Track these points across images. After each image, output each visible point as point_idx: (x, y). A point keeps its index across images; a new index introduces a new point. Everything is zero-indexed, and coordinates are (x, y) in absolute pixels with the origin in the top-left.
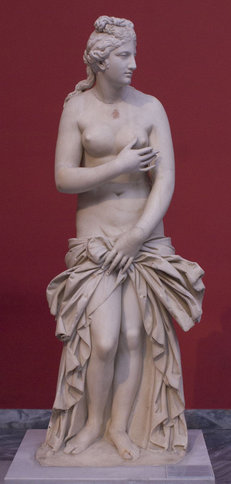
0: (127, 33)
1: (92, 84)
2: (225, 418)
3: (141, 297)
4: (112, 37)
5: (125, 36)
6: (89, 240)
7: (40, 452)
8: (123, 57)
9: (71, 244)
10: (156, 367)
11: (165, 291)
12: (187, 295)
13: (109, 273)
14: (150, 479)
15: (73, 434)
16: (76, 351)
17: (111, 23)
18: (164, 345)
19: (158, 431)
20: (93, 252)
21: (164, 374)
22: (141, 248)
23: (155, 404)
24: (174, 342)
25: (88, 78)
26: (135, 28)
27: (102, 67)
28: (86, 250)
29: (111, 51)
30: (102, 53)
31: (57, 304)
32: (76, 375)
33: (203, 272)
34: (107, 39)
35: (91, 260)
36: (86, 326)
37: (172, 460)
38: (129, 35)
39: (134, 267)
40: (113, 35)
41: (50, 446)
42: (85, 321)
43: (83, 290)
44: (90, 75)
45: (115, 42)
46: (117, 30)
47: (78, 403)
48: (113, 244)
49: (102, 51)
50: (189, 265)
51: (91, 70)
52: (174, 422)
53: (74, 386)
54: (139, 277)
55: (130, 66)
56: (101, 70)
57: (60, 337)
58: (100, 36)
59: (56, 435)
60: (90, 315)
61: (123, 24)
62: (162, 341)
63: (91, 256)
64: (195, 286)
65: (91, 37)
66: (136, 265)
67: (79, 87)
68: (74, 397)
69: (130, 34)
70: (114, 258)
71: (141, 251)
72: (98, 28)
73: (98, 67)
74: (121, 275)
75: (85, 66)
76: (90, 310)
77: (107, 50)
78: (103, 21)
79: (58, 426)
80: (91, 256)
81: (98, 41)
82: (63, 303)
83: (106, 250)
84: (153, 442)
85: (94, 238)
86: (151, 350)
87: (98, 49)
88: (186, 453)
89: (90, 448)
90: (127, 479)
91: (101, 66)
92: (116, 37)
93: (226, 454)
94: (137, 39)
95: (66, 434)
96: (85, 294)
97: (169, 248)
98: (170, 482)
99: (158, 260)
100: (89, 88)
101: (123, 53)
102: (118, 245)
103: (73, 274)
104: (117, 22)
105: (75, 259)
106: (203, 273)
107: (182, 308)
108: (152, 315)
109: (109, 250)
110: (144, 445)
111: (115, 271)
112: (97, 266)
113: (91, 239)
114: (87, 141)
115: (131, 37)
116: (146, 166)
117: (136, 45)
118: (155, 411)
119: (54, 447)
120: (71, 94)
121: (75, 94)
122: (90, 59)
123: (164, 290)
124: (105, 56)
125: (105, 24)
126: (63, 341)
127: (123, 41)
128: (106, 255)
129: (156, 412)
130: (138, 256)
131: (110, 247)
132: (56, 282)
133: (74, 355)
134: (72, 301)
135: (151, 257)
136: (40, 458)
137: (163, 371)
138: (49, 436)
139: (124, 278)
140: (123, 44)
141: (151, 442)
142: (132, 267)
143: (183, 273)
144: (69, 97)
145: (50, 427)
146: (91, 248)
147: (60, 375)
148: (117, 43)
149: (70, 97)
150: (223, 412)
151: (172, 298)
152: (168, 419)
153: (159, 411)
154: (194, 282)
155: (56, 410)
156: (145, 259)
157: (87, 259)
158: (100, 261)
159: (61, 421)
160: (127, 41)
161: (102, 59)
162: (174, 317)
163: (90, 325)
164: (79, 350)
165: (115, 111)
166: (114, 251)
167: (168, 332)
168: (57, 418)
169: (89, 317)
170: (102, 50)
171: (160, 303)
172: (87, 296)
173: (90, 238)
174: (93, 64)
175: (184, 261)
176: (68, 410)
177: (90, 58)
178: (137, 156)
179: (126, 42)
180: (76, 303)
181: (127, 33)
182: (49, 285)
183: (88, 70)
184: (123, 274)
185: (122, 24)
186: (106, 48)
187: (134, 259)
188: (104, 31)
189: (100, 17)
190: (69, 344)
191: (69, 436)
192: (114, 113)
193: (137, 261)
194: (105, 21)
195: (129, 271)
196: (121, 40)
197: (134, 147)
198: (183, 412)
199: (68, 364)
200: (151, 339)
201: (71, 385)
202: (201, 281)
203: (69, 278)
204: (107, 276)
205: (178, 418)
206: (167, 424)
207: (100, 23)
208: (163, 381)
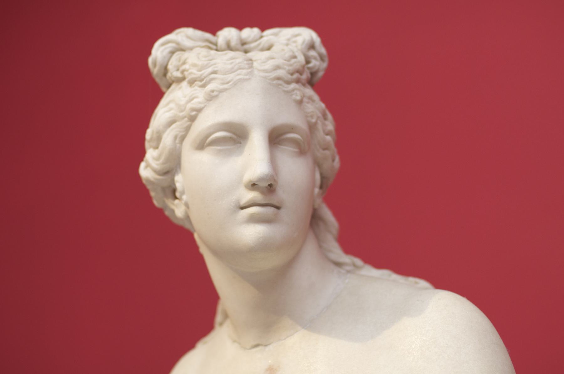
8: (219, 148)
29: (183, 138)
78: (163, 44)
91: (173, 204)
92: (192, 83)
124: (163, 163)
127: (210, 87)
148: (191, 100)
170: (154, 144)
179: (225, 90)
185: (259, 45)
186: (164, 132)
196: (204, 86)
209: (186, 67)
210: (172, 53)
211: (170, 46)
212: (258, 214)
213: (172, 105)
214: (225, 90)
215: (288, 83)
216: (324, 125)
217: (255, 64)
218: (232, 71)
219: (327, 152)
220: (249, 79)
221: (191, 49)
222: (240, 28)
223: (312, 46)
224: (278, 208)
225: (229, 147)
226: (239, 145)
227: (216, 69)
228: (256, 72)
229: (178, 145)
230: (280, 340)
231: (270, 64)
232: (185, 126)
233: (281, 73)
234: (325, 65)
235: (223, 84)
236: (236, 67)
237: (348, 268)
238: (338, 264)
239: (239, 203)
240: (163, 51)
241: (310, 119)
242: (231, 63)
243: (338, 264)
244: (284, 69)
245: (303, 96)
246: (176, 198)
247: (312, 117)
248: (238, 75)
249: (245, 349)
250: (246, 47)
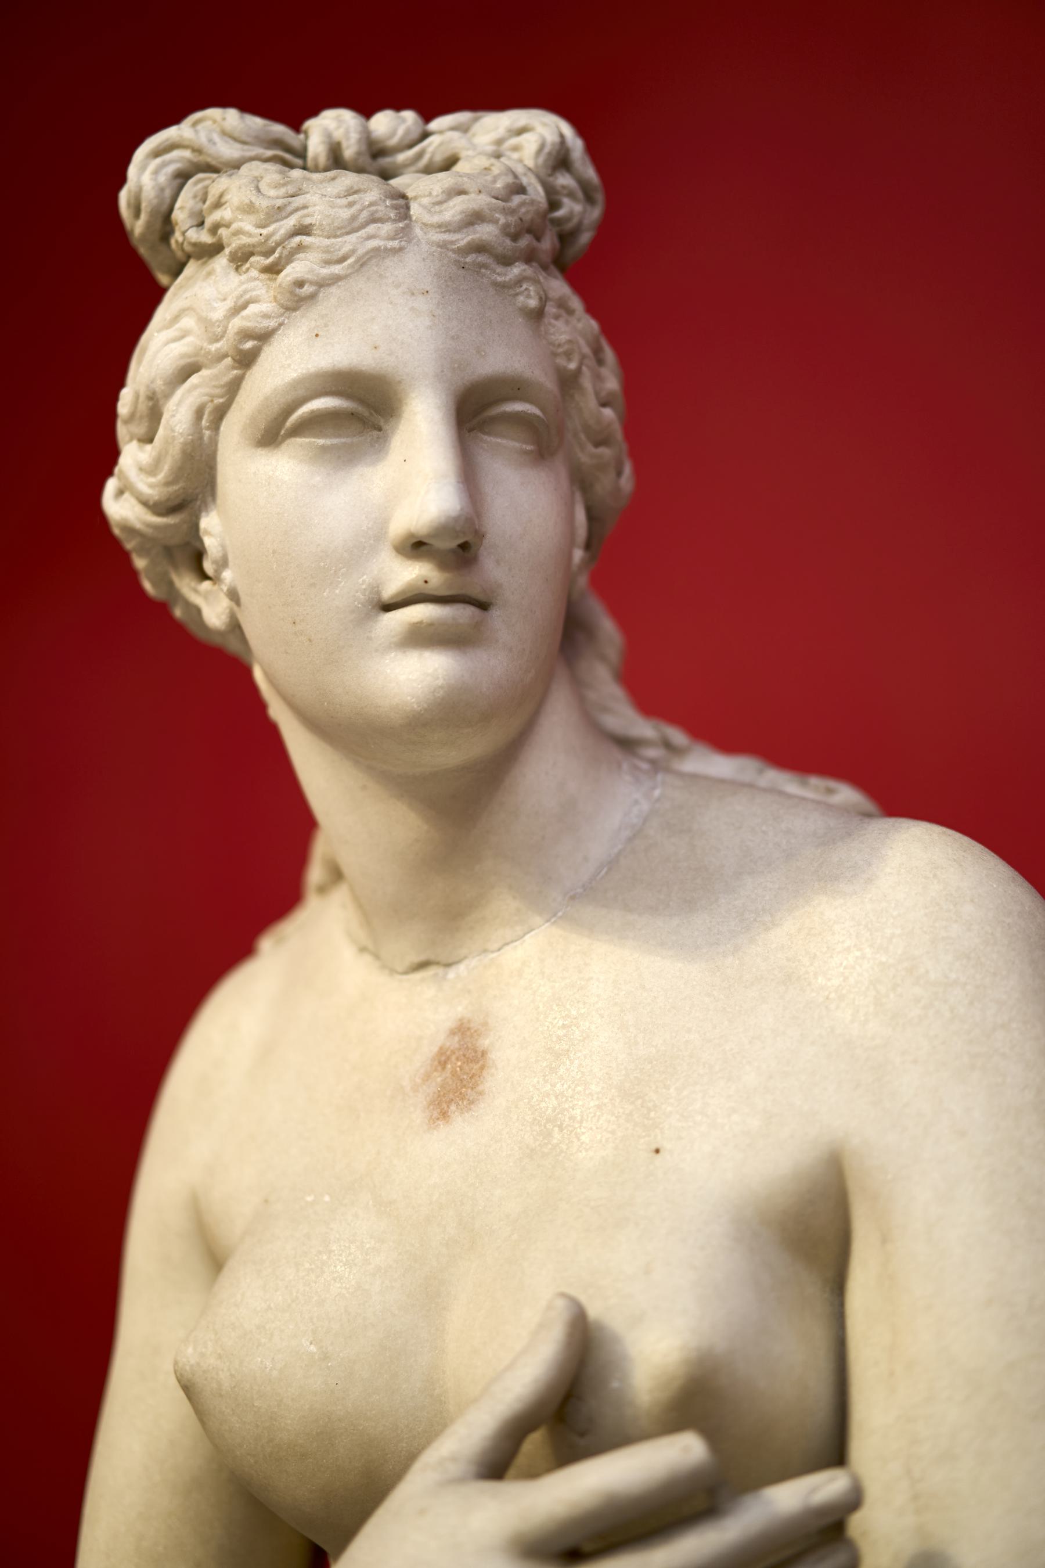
8: (321, 441)
29: (220, 413)
45: (218, 313)
49: (150, 440)
78: (157, 153)
92: (240, 259)
124: (167, 484)
127: (294, 271)
160: (343, 259)
170: (141, 429)
179: (336, 279)
185: (420, 156)
186: (168, 396)
192: (442, 1059)
194: (176, 154)
196: (273, 270)
209: (225, 214)
210: (183, 177)
211: (180, 157)
212: (431, 625)
213: (188, 322)
214: (336, 279)
215: (506, 261)
216: (598, 378)
217: (415, 210)
218: (351, 227)
219: (605, 452)
220: (401, 249)
221: (236, 165)
222: (367, 111)
223: (561, 161)
224: (483, 606)
225: (348, 440)
226: (375, 433)
227: (307, 221)
228: (418, 231)
229: (207, 433)
230: (485, 951)
231: (454, 209)
232: (226, 379)
233: (486, 232)
234: (595, 213)
235: (328, 263)
236: (365, 215)
237: (652, 753)
238: (627, 744)
239: (378, 593)
240: (156, 172)
241: (561, 361)
242: (351, 205)
243: (627, 744)
244: (496, 221)
245: (544, 300)
246: (204, 576)
247: (568, 355)
248: (370, 237)
249: (393, 971)
250: (385, 161)
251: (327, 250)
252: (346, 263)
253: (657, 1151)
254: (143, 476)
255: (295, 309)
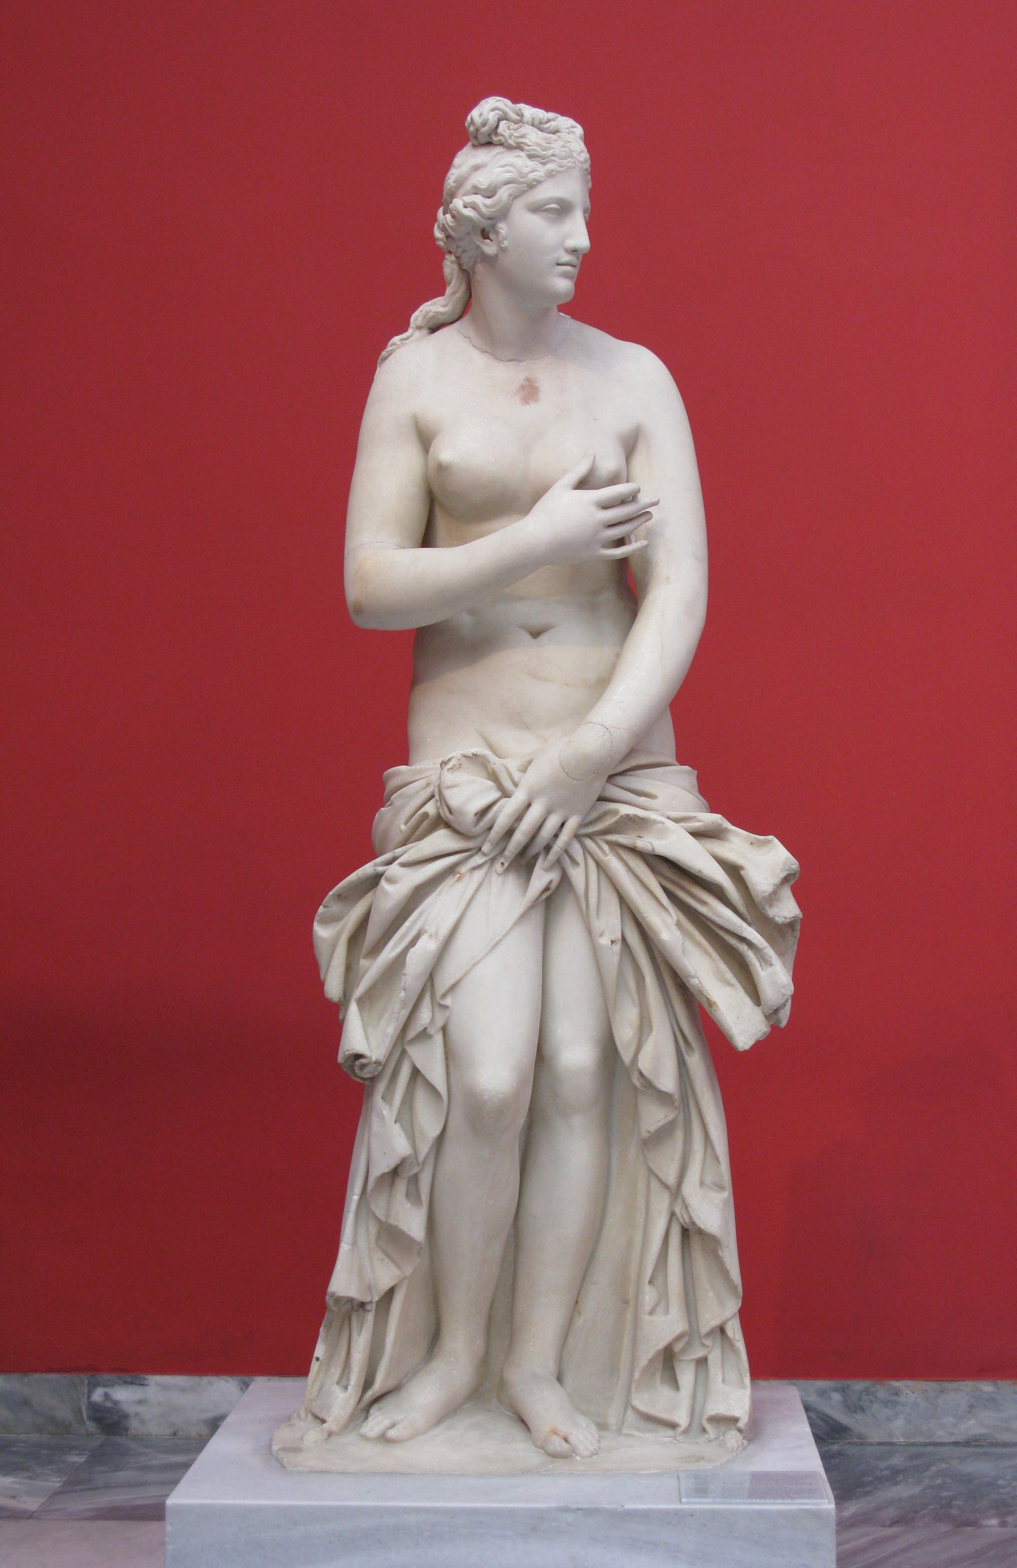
0: (563, 147)
1: (459, 309)
2: (876, 1406)
3: (604, 941)
4: (518, 156)
5: (557, 152)
6: (443, 765)
7: (284, 1435)
9: (390, 785)
10: (650, 1171)
11: (678, 924)
12: (744, 935)
13: (506, 865)
14: (629, 1506)
15: (391, 1383)
16: (399, 1112)
17: (514, 116)
18: (676, 1097)
19: (658, 1376)
20: (455, 798)
21: (676, 1192)
22: (603, 789)
23: (647, 1288)
24: (705, 1088)
25: (449, 291)
26: (588, 140)
27: (490, 248)
28: (437, 797)
29: (516, 197)
30: (488, 202)
31: (344, 967)
32: (401, 1187)
33: (794, 864)
34: (501, 163)
35: (448, 825)
36: (431, 1031)
37: (700, 1459)
38: (568, 150)
39: (580, 851)
40: (522, 149)
41: (316, 1417)
42: (431, 1016)
43: (423, 918)
44: (454, 281)
45: (526, 170)
46: (533, 137)
47: (406, 1282)
48: (517, 775)
50: (752, 844)
51: (455, 267)
52: (708, 1347)
53: (396, 1223)
54: (599, 881)
55: (571, 243)
56: (485, 258)
57: (352, 1067)
58: (482, 156)
59: (336, 1381)
60: (444, 996)
61: (553, 124)
62: (667, 1082)
63: (451, 812)
64: (771, 905)
65: (457, 161)
66: (588, 842)
67: (420, 319)
68: (395, 1263)
69: (570, 150)
70: (519, 818)
71: (602, 799)
72: (477, 130)
73: (478, 247)
74: (542, 872)
75: (439, 255)
76: (445, 979)
77: (503, 194)
78: (493, 110)
79: (343, 1353)
80: (451, 812)
81: (477, 168)
82: (363, 962)
83: (495, 795)
84: (642, 1408)
85: (459, 756)
86: (635, 1116)
87: (476, 191)
88: (745, 1442)
89: (442, 1427)
90: (553, 1505)
91: (484, 244)
92: (531, 157)
93: (879, 1509)
94: (592, 166)
95: (368, 1383)
96: (431, 930)
97: (691, 795)
98: (691, 1515)
99: (660, 825)
100: (450, 321)
101: (552, 203)
102: (530, 780)
103: (394, 869)
104: (533, 119)
105: (403, 827)
106: (793, 867)
107: (729, 975)
108: (637, 1002)
109: (506, 794)
110: (612, 1420)
111: (524, 862)
112: (470, 844)
113: (450, 760)
114: (442, 468)
115: (573, 157)
116: (620, 542)
117: (590, 185)
118: (647, 1307)
119: (330, 1419)
120: (396, 339)
121: (408, 338)
122: (452, 224)
123: (675, 918)
124: (494, 212)
125: (496, 119)
126: (363, 1078)
127: (550, 166)
128: (496, 808)
129: (651, 1313)
130: (594, 815)
131: (508, 784)
132: (340, 897)
133: (395, 1122)
134: (390, 952)
135: (636, 816)
136: (285, 1449)
137: (671, 1179)
138: (316, 1387)
139: (551, 882)
140: (551, 175)
141: (636, 1410)
142: (577, 850)
143: (734, 871)
144: (390, 348)
145: (318, 1359)
146: (446, 788)
147: (352, 1191)
148: (532, 171)
149: (394, 347)
150: (867, 1389)
151: (699, 945)
152: (689, 1336)
153: (659, 1309)
154: (766, 894)
155: (338, 1300)
156: (616, 822)
157: (441, 822)
158: (477, 828)
159: (355, 1335)
160: (563, 167)
161: (489, 222)
162: (705, 1006)
163: (444, 1029)
164: (411, 1108)
165: (525, 383)
166: (519, 797)
167: (688, 1055)
168: (341, 1329)
169: (442, 1002)
170: (488, 195)
171: (659, 961)
172: (436, 933)
173: (447, 758)
174: (460, 239)
175: (735, 832)
176: (378, 1303)
177: (452, 220)
178: (593, 509)
179: (561, 172)
180: (400, 960)
181: (563, 147)
182: (321, 907)
183: (449, 267)
184: (548, 870)
185: (550, 127)
186: (500, 188)
187: (584, 825)
188: (495, 139)
189: (483, 103)
190: (381, 1087)
191: (377, 1387)
192: (523, 387)
193: (590, 830)
194: (497, 112)
195: (567, 861)
196: (544, 164)
197: (583, 484)
198: (734, 1316)
199: (377, 1154)
200: (636, 1081)
201: (383, 1219)
202: (787, 894)
203: (383, 883)
204: (499, 875)
205: (718, 1333)
206: (684, 1350)
207: (482, 117)
208: (672, 1215)
217: (574, 154)
227: (555, 153)
229: (511, 202)
235: (560, 167)
240: (494, 117)
242: (565, 151)
249: (501, 360)
250: (542, 126)
251: (560, 163)
252: (565, 168)
253: (596, 420)
254: (485, 207)
255: (549, 177)
